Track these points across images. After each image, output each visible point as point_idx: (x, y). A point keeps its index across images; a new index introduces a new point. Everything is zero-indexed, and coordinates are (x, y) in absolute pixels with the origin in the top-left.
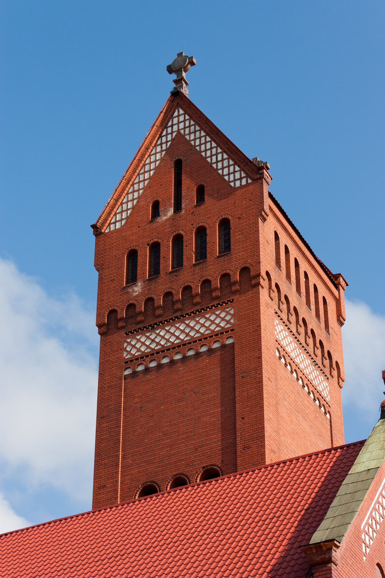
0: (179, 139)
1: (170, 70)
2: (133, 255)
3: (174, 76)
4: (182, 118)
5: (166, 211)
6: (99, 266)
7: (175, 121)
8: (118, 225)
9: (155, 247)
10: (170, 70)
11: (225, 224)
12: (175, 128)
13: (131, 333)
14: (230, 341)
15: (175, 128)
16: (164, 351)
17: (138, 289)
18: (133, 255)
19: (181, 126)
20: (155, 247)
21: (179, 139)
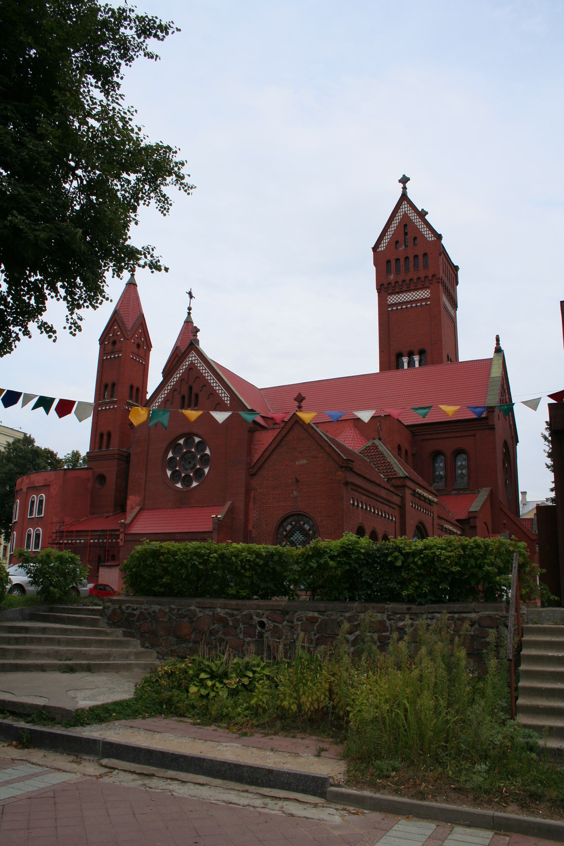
0: (405, 215)
1: (400, 181)
2: (389, 262)
3: (401, 185)
4: (406, 206)
5: (401, 246)
6: (376, 264)
7: (403, 207)
8: (382, 249)
9: (397, 260)
10: (400, 181)
11: (425, 255)
12: (404, 210)
13: (391, 294)
14: (429, 303)
15: (404, 210)
16: (403, 303)
17: (392, 277)
18: (389, 262)
19: (406, 209)
20: (397, 260)
21: (405, 215)
